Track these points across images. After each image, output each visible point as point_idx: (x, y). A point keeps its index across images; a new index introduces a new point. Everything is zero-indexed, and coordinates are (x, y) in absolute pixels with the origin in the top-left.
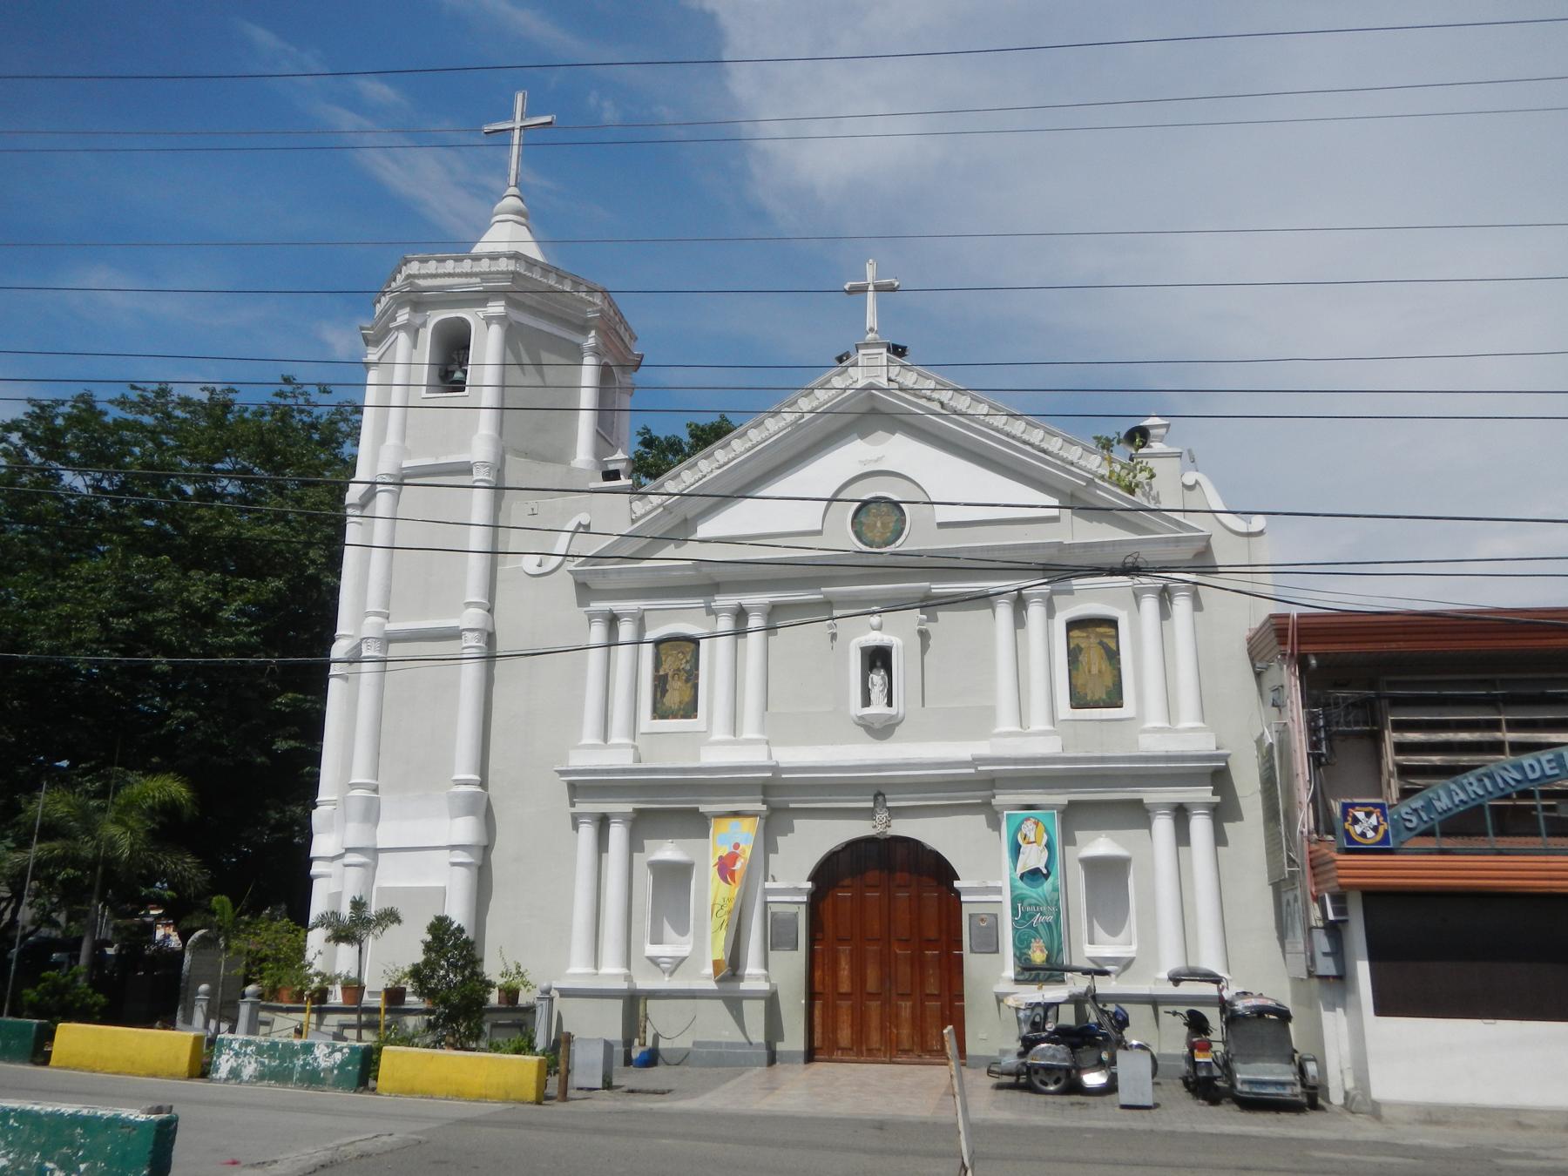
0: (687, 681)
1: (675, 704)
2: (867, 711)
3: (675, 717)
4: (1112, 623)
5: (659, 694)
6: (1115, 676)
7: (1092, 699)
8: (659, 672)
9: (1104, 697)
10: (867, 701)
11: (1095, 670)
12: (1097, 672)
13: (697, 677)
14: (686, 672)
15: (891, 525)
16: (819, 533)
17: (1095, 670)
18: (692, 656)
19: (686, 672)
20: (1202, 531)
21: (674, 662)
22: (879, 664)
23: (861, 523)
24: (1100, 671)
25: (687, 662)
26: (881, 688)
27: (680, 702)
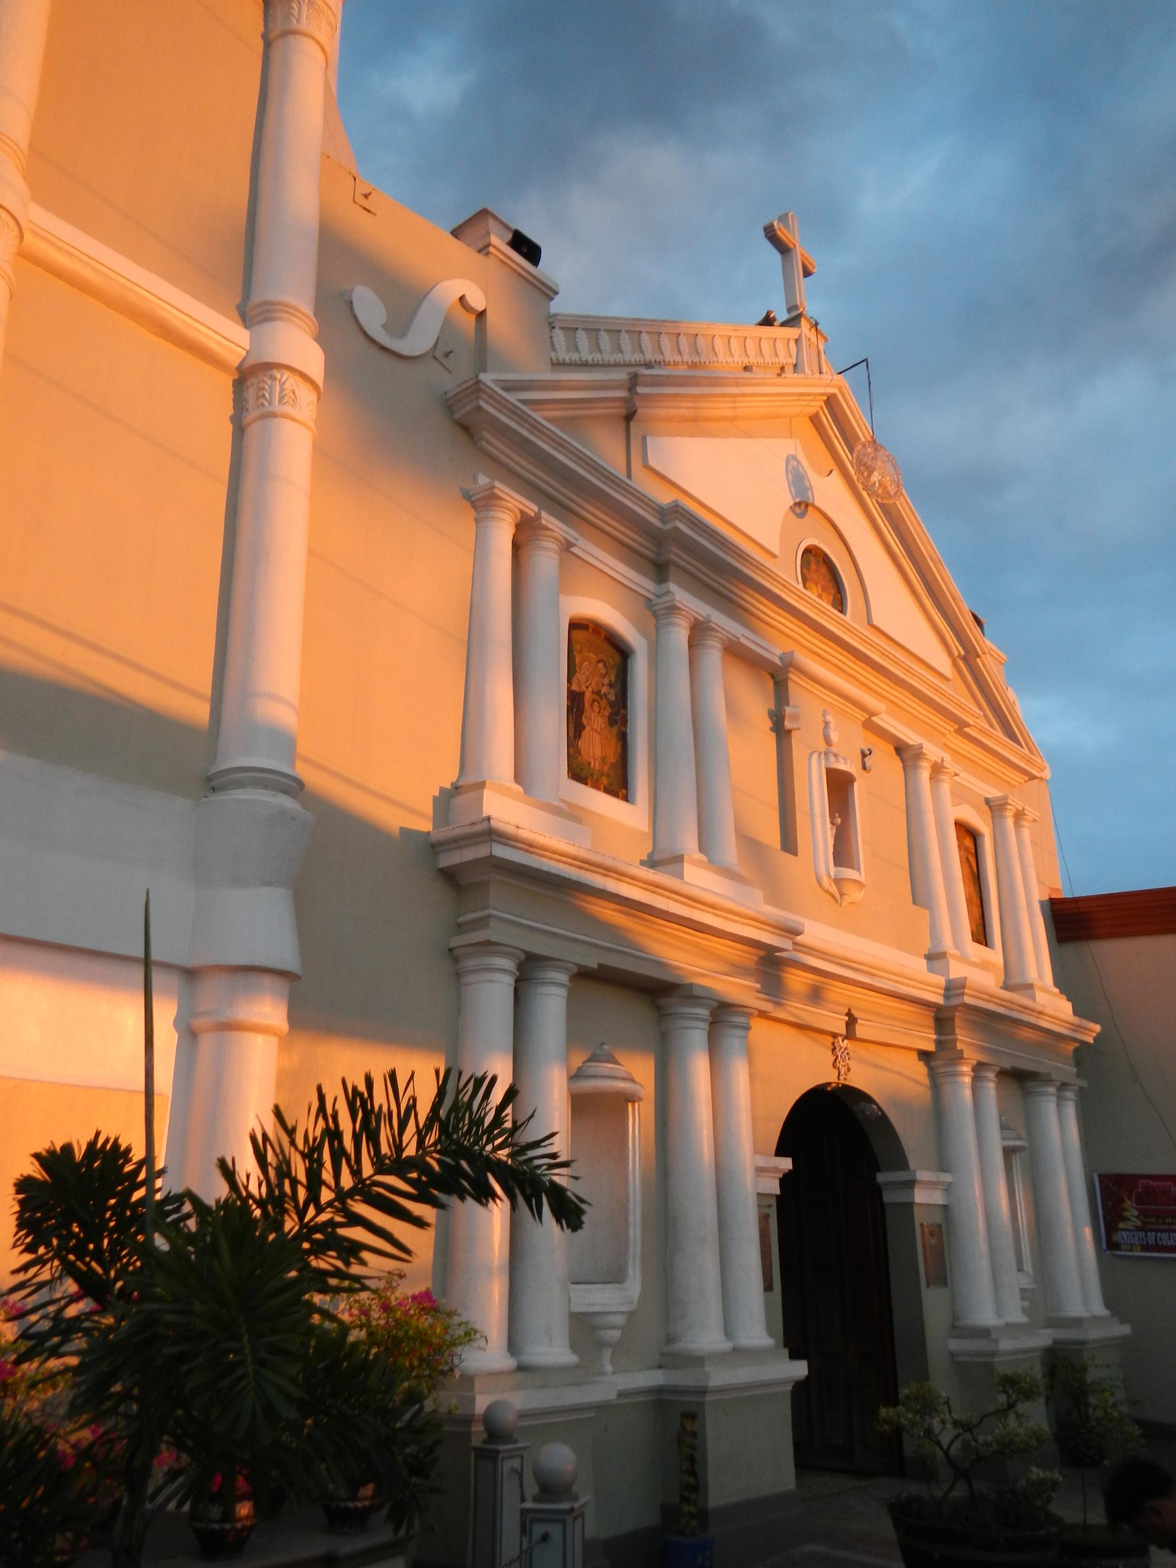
0: (612, 721)
3: (596, 786)
8: (571, 685)
18: (617, 676)
19: (611, 704)
25: (611, 685)
27: (603, 759)
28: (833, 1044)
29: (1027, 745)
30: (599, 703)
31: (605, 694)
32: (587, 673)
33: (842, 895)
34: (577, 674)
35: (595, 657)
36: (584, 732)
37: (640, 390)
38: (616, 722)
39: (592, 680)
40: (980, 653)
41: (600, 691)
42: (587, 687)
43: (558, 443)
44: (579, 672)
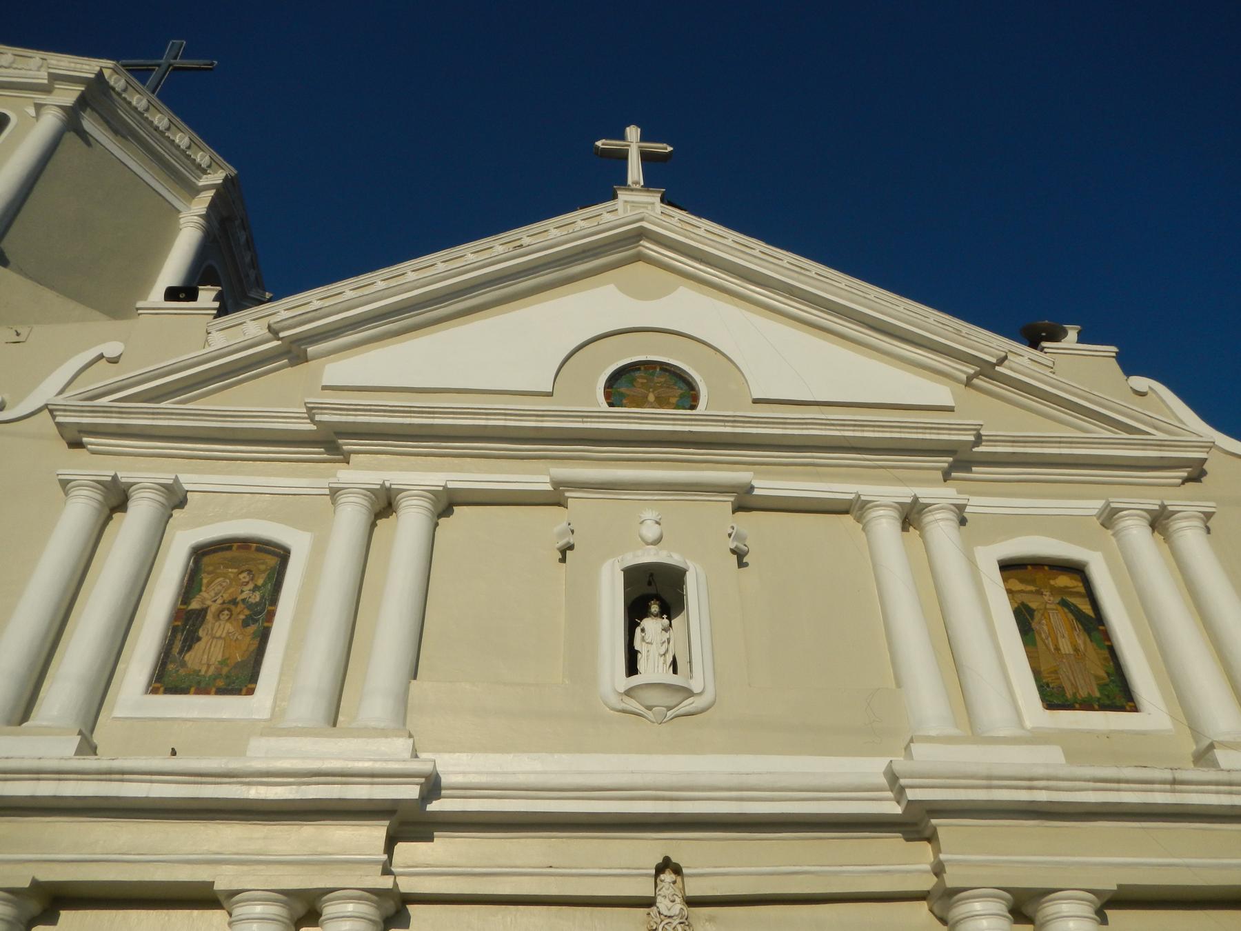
0: (245, 623)
1: (209, 666)
2: (635, 680)
3: (202, 690)
4: (1077, 570)
5: (178, 645)
6: (1105, 659)
7: (1074, 694)
9: (1098, 695)
10: (632, 669)
11: (1066, 647)
12: (1072, 652)
13: (271, 616)
14: (250, 606)
15: (674, 400)
16: (550, 394)
17: (1066, 647)
18: (269, 578)
20: (1201, 437)
21: (230, 585)
22: (655, 608)
23: (622, 395)
24: (1076, 650)
25: (256, 588)
26: (662, 651)
27: (223, 662)
28: (649, 914)
29: (1156, 428)
30: (229, 610)
31: (243, 600)
32: (219, 587)
33: (649, 708)
34: (204, 594)
35: (235, 571)
36: (198, 643)
37: (282, 335)
38: (256, 621)
39: (224, 593)
40: (994, 360)
41: (236, 599)
42: (215, 601)
43: (153, 414)
44: (205, 591)
